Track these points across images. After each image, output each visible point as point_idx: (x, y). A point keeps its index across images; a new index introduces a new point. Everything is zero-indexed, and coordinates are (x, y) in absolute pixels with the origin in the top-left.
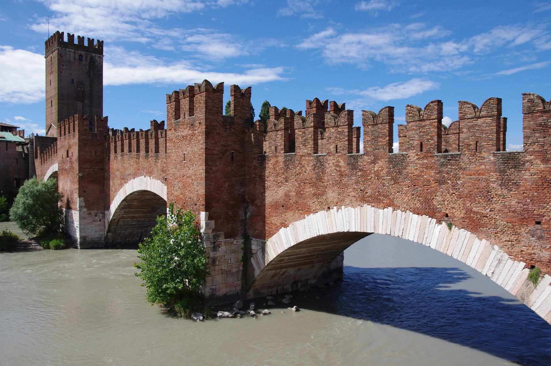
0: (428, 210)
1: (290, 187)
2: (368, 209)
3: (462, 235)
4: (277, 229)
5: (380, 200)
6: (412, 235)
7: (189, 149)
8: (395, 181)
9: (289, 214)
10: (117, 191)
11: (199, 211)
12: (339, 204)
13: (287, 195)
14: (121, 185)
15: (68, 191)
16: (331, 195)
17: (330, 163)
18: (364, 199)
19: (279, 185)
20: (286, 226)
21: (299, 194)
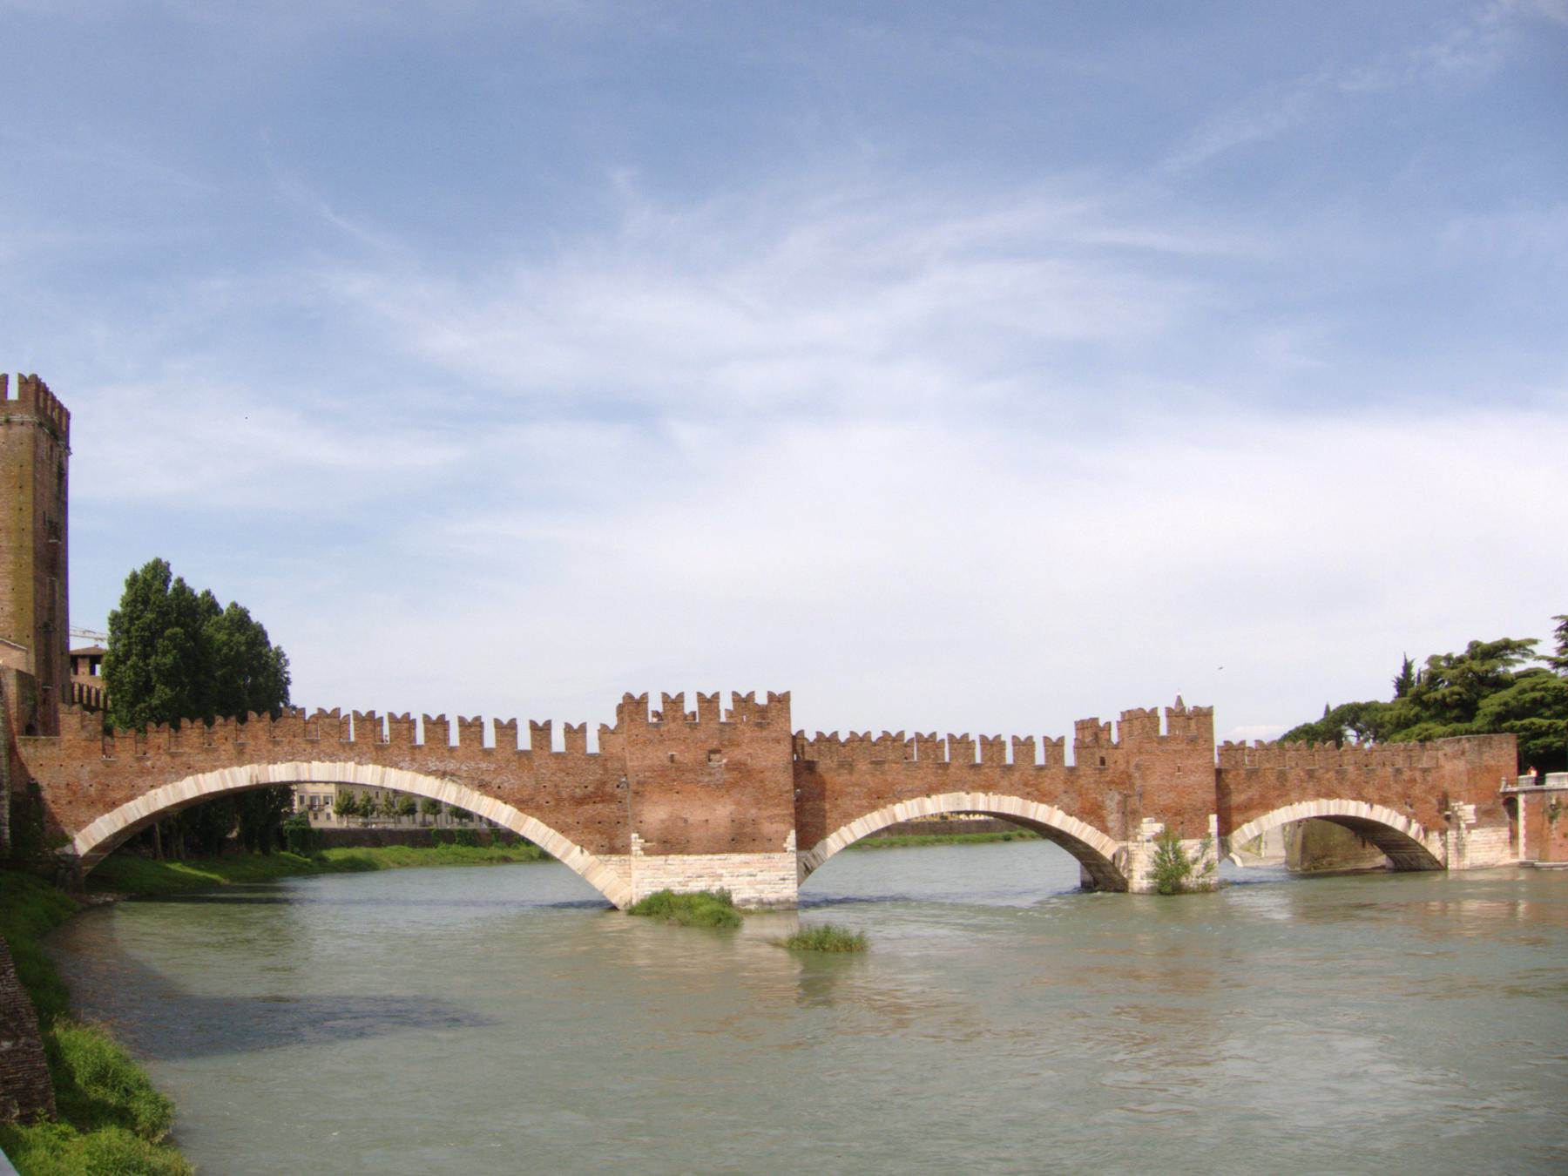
0: (1359, 797)
1: (1253, 792)
2: (1323, 802)
4: (1239, 825)
5: (1330, 794)
8: (1340, 783)
9: (1253, 813)
10: (848, 817)
11: (1207, 815)
12: (1300, 801)
13: (1251, 799)
14: (873, 808)
16: (1293, 795)
17: (1292, 775)
18: (1318, 795)
19: (1242, 792)
20: (1248, 821)
21: (1262, 797)
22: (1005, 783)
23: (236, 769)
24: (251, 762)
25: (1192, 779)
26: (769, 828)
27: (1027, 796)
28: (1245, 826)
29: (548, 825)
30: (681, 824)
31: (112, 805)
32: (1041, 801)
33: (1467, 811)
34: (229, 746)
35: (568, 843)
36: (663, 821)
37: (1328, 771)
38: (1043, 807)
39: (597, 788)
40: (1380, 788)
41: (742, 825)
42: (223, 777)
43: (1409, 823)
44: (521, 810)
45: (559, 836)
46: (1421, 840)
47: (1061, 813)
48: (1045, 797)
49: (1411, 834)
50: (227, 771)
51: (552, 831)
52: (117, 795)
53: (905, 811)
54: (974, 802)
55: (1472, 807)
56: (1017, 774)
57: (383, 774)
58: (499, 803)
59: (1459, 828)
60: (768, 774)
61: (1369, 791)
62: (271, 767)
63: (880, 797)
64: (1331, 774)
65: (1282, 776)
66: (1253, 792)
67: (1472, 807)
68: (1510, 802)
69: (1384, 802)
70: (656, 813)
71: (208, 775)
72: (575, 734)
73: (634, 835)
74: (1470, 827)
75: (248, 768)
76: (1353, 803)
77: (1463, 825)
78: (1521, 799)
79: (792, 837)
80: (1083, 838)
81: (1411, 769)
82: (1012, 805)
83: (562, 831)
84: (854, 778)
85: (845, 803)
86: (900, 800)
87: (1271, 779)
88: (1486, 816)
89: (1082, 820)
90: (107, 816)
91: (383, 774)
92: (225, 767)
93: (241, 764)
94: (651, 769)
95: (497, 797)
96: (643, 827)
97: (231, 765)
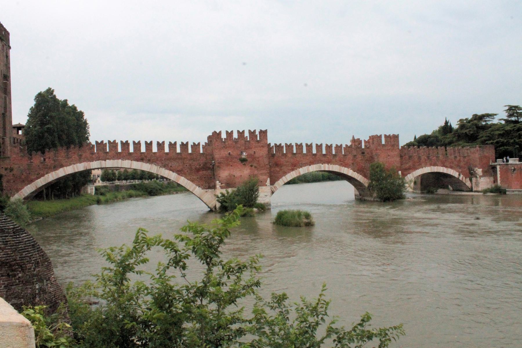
0: (444, 166)
2: (432, 167)
3: (450, 169)
4: (406, 175)
6: (441, 171)
7: (392, 153)
9: (411, 171)
12: (425, 167)
13: (410, 166)
14: (293, 170)
16: (423, 165)
18: (431, 165)
21: (414, 165)
22: (334, 160)
23: (78, 164)
24: (84, 162)
26: (261, 178)
27: (341, 165)
28: (408, 175)
29: (188, 179)
31: (32, 181)
32: (345, 167)
33: (479, 171)
34: (76, 156)
35: (194, 185)
36: (227, 176)
37: (433, 157)
38: (346, 168)
39: (204, 165)
40: (450, 163)
42: (74, 169)
43: (459, 175)
44: (179, 174)
45: (191, 183)
47: (351, 171)
48: (346, 165)
49: (461, 178)
50: (75, 166)
51: (189, 181)
52: (33, 177)
53: (303, 171)
54: (324, 167)
55: (481, 170)
56: (338, 157)
58: (171, 172)
59: (476, 177)
60: (260, 159)
61: (447, 164)
62: (91, 163)
63: (295, 166)
64: (435, 158)
65: (419, 158)
66: (410, 164)
67: (481, 170)
68: (494, 168)
69: (451, 167)
71: (68, 167)
72: (196, 146)
73: (218, 182)
74: (480, 177)
75: (83, 164)
76: (442, 168)
77: (478, 176)
78: (498, 167)
79: (269, 180)
80: (358, 179)
81: (460, 156)
82: (336, 168)
83: (192, 181)
84: (287, 159)
85: (284, 168)
86: (301, 167)
87: (416, 159)
88: (485, 173)
89: (358, 173)
90: (29, 186)
92: (74, 164)
93: (80, 162)
94: (222, 158)
95: (170, 170)
97: (77, 163)
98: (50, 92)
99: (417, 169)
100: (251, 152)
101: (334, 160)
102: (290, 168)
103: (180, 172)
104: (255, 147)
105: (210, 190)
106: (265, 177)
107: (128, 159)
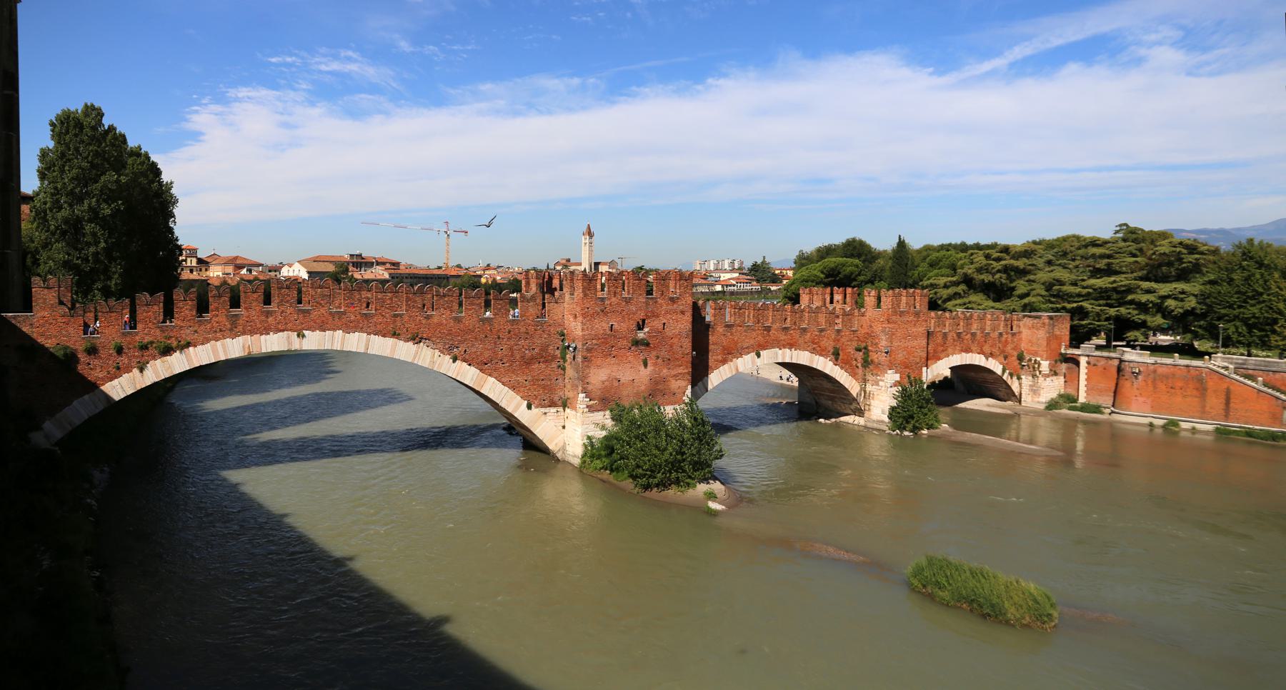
5: (968, 350)
14: (724, 362)
15: (646, 381)
16: (950, 350)
24: (244, 333)
25: (915, 343)
26: (675, 385)
27: (813, 351)
30: (616, 384)
41: (657, 383)
42: (215, 351)
43: (1004, 371)
45: (511, 393)
46: (1009, 382)
48: (821, 352)
49: (1005, 377)
50: (219, 343)
57: (368, 341)
60: (675, 340)
61: (987, 349)
70: (599, 376)
71: (200, 348)
83: (513, 388)
86: (741, 355)
90: (86, 397)
91: (368, 341)
92: (217, 340)
94: (596, 337)
96: (590, 387)
98: (94, 113)
99: (939, 359)
100: (657, 324)
101: (801, 341)
102: (720, 358)
103: (484, 365)
104: (667, 312)
105: (553, 410)
106: (682, 383)
107: (361, 330)
